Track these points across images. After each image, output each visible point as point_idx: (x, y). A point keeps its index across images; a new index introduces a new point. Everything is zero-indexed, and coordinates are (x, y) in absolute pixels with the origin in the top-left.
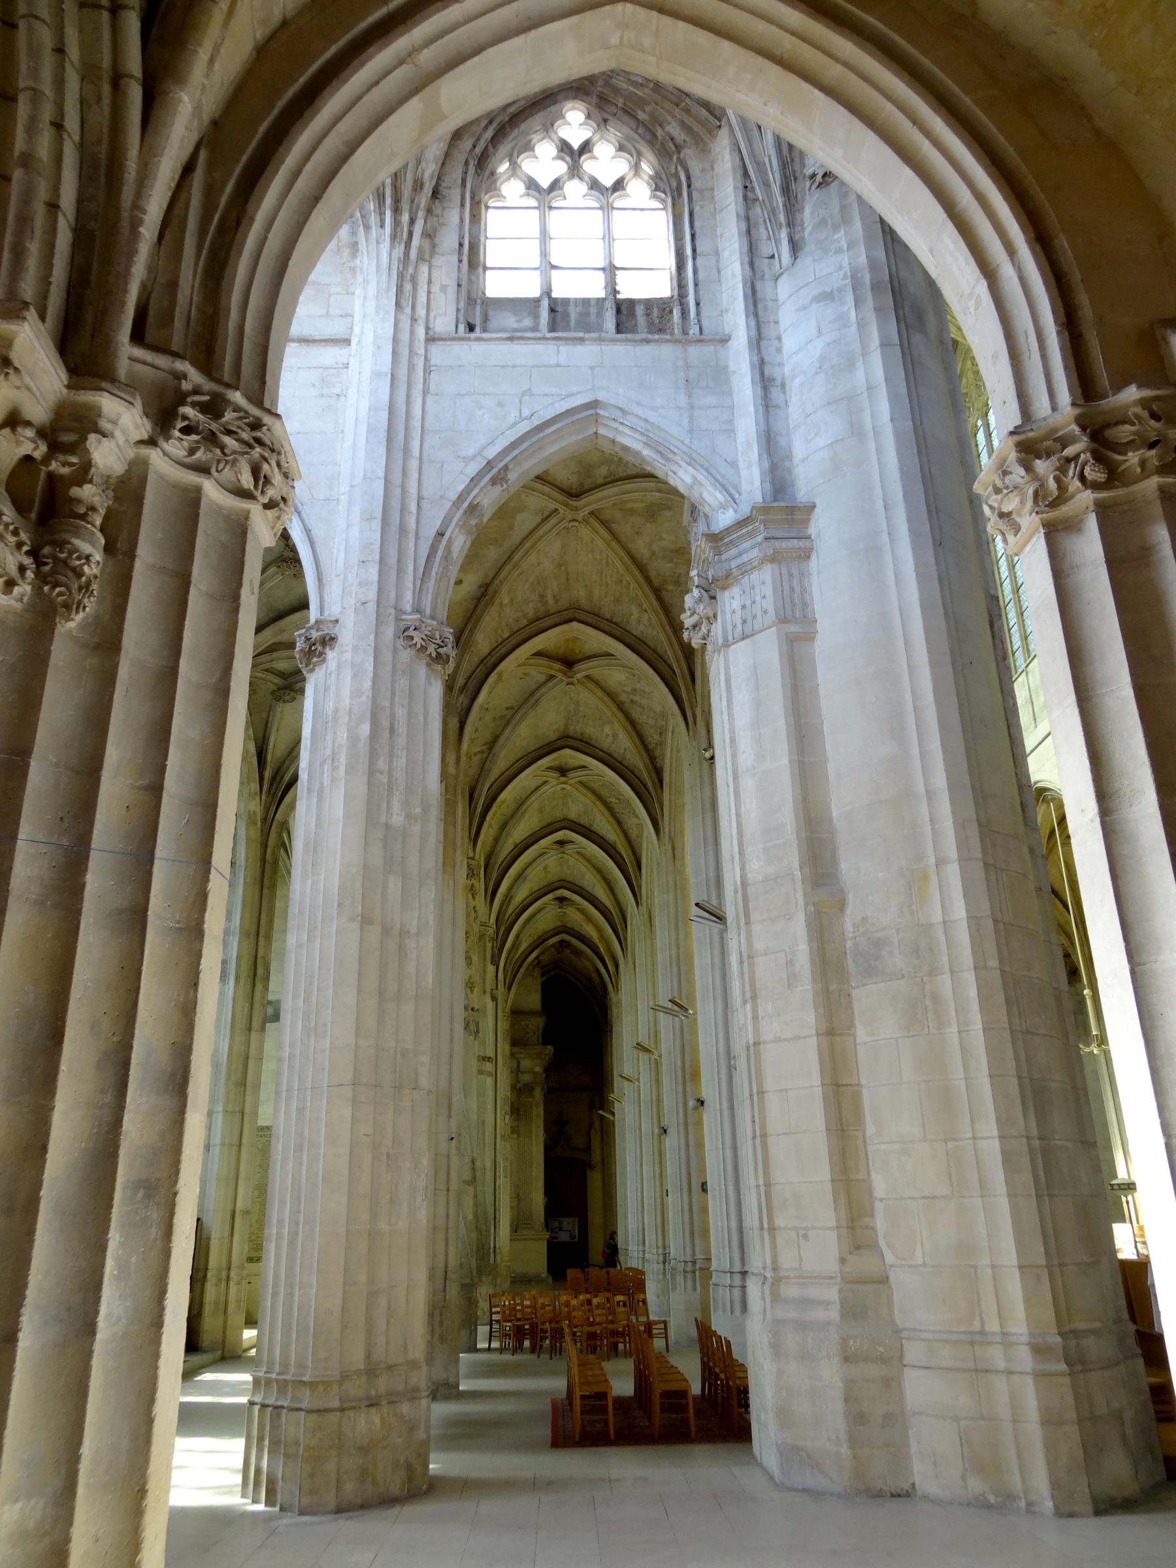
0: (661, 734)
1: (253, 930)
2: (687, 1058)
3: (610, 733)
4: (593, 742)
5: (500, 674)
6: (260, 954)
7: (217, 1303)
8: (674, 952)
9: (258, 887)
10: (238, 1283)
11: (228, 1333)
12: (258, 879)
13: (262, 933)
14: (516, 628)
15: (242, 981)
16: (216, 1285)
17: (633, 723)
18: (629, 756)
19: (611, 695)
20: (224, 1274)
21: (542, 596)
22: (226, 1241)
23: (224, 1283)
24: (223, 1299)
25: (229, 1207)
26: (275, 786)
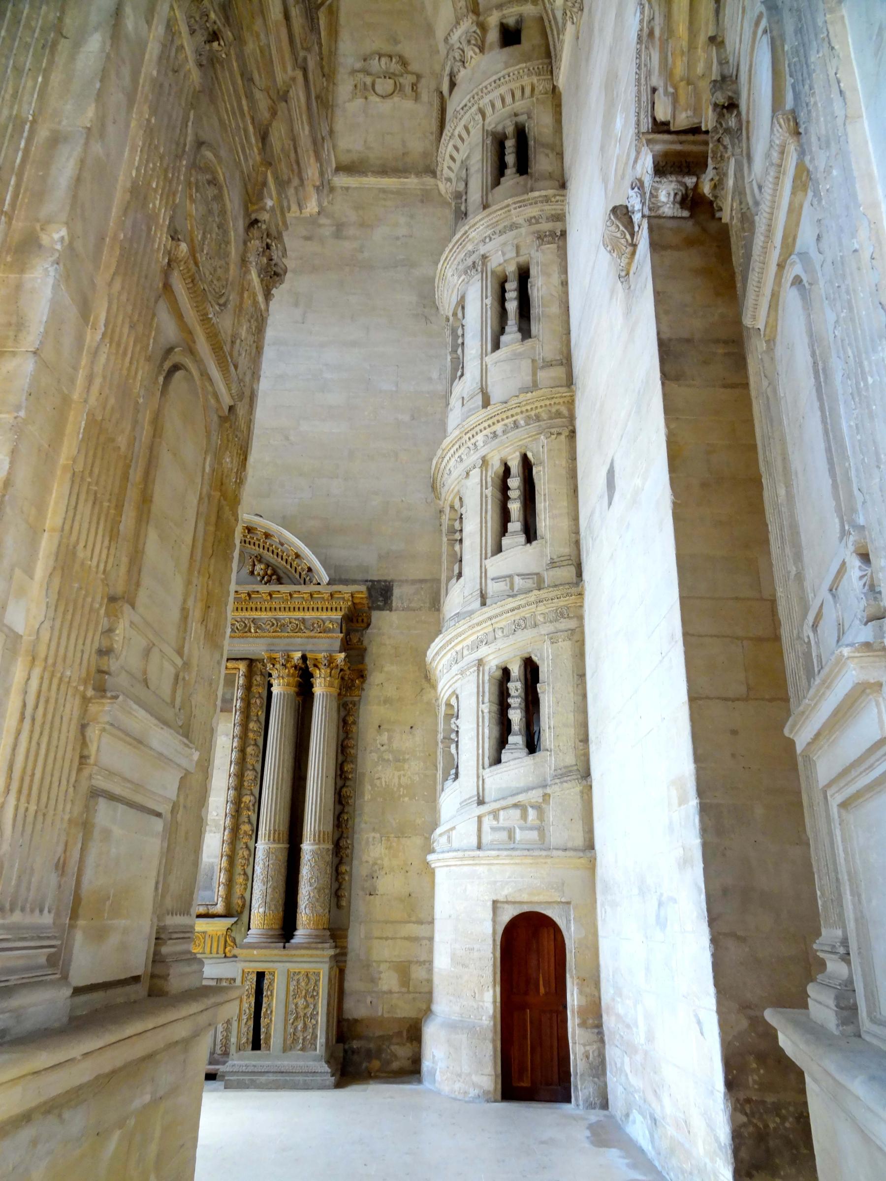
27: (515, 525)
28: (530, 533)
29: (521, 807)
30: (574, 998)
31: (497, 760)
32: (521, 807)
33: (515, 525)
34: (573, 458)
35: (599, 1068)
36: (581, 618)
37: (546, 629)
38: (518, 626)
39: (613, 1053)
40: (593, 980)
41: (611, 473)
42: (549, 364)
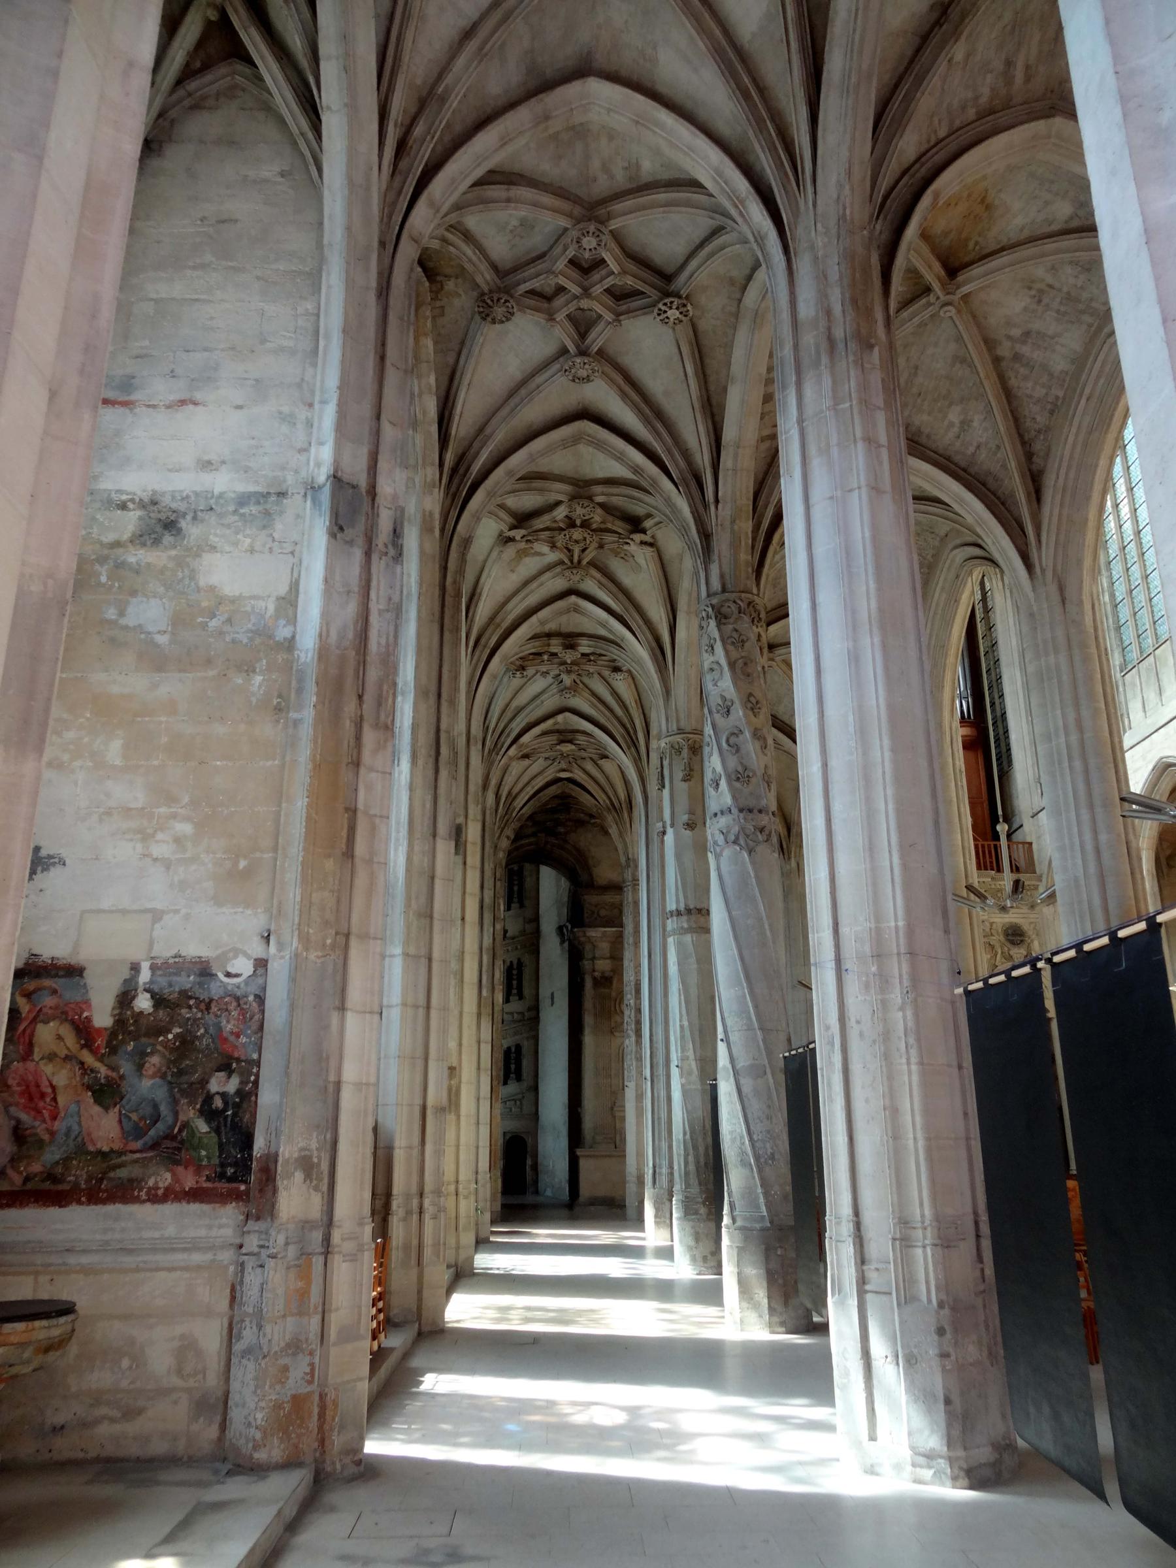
0: (1052, 412)
1: (433, 688)
2: (1111, 893)
3: (957, 422)
4: (923, 440)
5: (936, 195)
6: (443, 726)
7: (407, 1247)
8: (1074, 738)
9: (436, 627)
10: (435, 1217)
11: (425, 1294)
12: (437, 615)
13: (444, 695)
14: (957, 123)
15: (420, 762)
16: (405, 1219)
17: (1008, 394)
18: (983, 455)
19: (989, 343)
20: (415, 1202)
21: (1009, 63)
22: (415, 1152)
23: (415, 1217)
24: (415, 1242)
25: (418, 1101)
26: (456, 481)
27: (515, 991)
28: (521, 996)
29: (515, 1101)
30: (529, 1162)
31: (505, 1083)
32: (515, 1101)
33: (515, 991)
34: (538, 963)
35: (536, 1182)
36: (537, 1030)
37: (525, 1035)
38: (515, 1034)
39: (541, 1176)
40: (535, 1156)
41: (552, 994)
42: (530, 921)
